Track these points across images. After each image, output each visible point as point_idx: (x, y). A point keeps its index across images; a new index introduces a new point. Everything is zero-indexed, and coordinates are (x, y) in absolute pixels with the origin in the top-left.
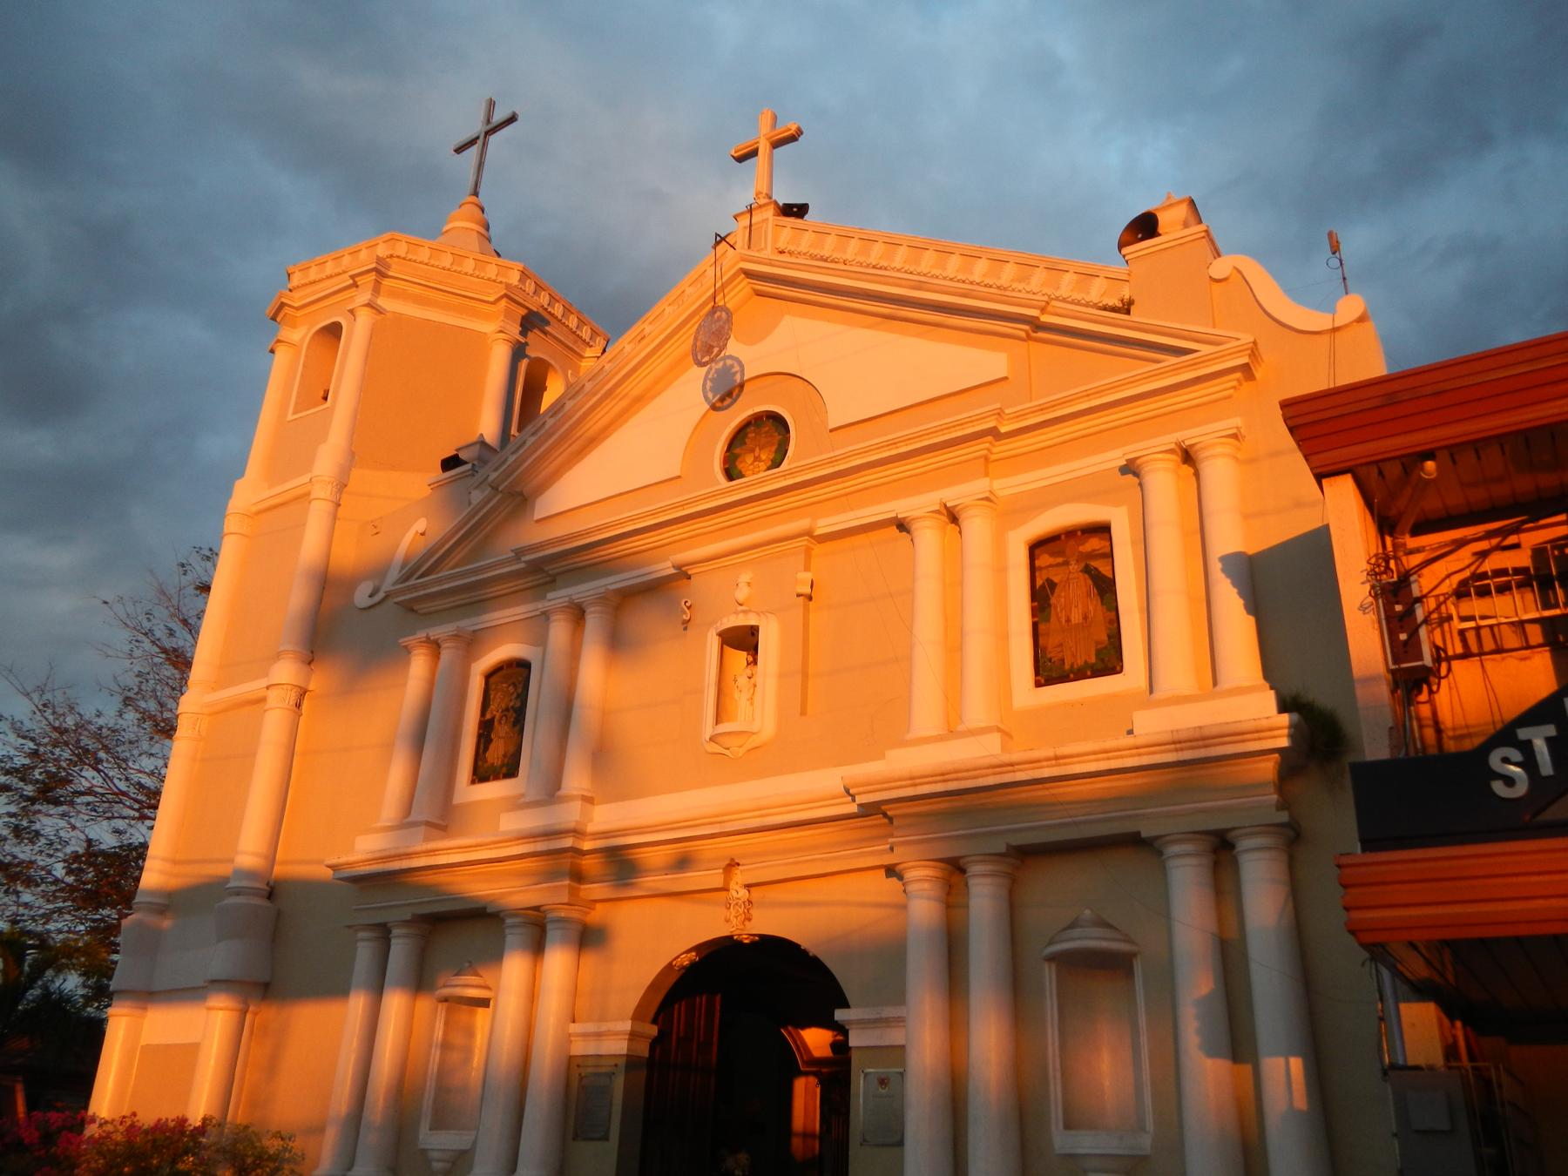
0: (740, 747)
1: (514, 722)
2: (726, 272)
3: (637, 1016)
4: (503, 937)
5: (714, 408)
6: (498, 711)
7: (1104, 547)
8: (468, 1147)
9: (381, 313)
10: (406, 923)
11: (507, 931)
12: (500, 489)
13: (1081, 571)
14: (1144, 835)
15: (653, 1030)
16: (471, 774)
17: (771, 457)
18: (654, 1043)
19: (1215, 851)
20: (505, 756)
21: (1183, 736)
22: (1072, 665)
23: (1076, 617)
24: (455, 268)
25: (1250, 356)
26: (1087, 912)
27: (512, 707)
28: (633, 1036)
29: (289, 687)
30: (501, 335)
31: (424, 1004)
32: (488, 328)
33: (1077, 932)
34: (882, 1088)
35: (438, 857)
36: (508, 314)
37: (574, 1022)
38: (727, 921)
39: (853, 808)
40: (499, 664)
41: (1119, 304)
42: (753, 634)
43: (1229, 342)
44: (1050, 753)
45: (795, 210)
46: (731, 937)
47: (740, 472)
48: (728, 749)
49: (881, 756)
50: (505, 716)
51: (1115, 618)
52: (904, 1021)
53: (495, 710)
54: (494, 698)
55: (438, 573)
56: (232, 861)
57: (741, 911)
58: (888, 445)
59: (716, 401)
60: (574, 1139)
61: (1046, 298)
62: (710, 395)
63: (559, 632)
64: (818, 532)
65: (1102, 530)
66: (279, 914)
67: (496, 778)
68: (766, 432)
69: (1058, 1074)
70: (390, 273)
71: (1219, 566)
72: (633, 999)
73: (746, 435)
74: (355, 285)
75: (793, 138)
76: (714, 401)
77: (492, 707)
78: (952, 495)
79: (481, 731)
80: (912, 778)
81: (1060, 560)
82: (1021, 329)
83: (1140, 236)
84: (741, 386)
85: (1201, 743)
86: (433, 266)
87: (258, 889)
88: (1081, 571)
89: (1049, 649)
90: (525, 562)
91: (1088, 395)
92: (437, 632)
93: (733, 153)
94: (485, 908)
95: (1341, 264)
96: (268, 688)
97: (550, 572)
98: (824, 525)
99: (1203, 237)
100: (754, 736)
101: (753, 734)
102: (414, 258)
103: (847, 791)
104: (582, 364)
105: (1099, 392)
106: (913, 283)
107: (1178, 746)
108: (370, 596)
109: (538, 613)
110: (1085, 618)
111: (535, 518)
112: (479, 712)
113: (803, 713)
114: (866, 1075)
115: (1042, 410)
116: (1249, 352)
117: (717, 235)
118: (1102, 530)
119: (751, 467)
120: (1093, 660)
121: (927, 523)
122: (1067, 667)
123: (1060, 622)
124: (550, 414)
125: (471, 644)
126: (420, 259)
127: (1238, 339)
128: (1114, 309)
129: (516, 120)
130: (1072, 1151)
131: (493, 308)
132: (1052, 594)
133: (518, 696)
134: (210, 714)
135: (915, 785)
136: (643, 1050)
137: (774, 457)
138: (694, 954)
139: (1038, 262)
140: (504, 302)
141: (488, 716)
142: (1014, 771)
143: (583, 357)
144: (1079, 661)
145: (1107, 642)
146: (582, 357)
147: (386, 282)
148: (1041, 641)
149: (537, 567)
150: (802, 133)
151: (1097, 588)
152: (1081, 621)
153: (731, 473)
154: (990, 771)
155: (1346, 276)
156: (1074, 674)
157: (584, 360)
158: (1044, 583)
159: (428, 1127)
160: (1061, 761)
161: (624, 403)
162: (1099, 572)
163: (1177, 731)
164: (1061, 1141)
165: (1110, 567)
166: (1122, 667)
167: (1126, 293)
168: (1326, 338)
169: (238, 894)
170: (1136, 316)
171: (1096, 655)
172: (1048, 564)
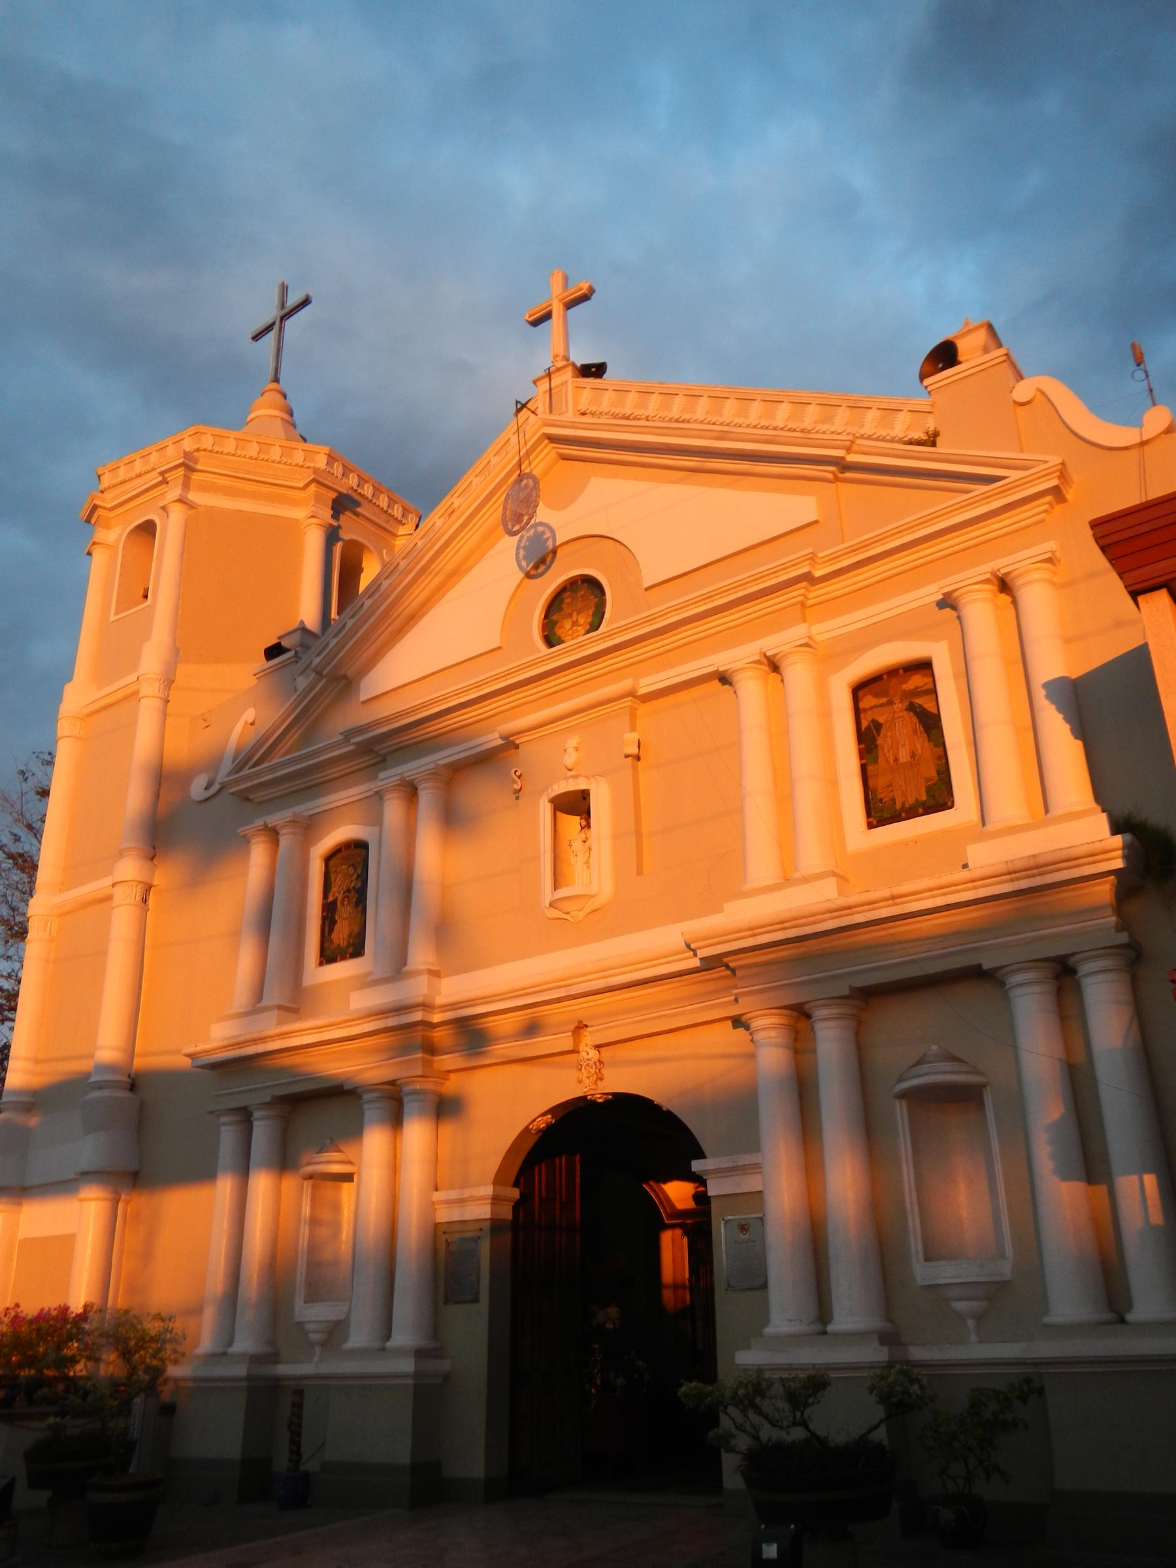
0: (580, 910)
2: (530, 439)
3: (498, 1181)
4: (361, 1113)
5: (528, 576)
6: (340, 892)
7: (928, 683)
8: (343, 1318)
9: (194, 508)
10: (265, 1105)
11: (366, 1106)
12: (324, 673)
13: (906, 710)
14: (986, 966)
15: (515, 1193)
17: (589, 620)
18: (517, 1206)
19: (1058, 977)
20: (350, 936)
21: (1018, 865)
22: (904, 803)
23: (904, 756)
24: (262, 456)
25: (1059, 478)
26: (934, 1047)
27: (353, 887)
28: (496, 1200)
29: (134, 884)
30: (313, 520)
31: (290, 1183)
32: (300, 513)
33: (926, 1067)
34: (744, 1234)
35: (292, 1039)
36: (318, 498)
37: (437, 1190)
38: (580, 1082)
39: (695, 963)
40: (337, 846)
41: (925, 437)
42: (584, 798)
43: (1038, 465)
44: (886, 893)
45: (593, 370)
46: (585, 1097)
47: (560, 638)
48: (568, 913)
49: (721, 910)
50: (347, 897)
51: (943, 753)
52: (760, 1168)
53: (336, 892)
54: (335, 880)
55: (270, 761)
56: (92, 1056)
57: (593, 1071)
58: (704, 599)
59: (530, 569)
60: (445, 1303)
61: (850, 437)
62: (524, 564)
63: (393, 810)
64: (641, 692)
65: (924, 666)
66: (142, 1106)
67: (343, 958)
68: (582, 596)
69: (916, 1208)
70: (199, 467)
71: (1043, 692)
72: (494, 1164)
73: (562, 601)
74: (165, 482)
75: (585, 298)
76: (528, 569)
78: (771, 643)
79: (325, 914)
80: (751, 929)
81: (884, 700)
82: (828, 471)
83: (940, 366)
84: (554, 552)
85: (1035, 871)
86: (240, 456)
87: (120, 1082)
88: (906, 710)
89: (880, 790)
90: (354, 744)
91: (899, 532)
92: (274, 819)
93: (527, 317)
94: (341, 1086)
95: (1147, 376)
96: (113, 885)
97: (380, 752)
98: (647, 685)
99: (1005, 361)
100: (594, 899)
101: (592, 896)
102: (221, 450)
103: (688, 946)
104: (397, 543)
105: (910, 528)
106: (717, 434)
107: (1013, 876)
108: (206, 789)
109: (371, 793)
110: (913, 756)
111: (362, 699)
113: (640, 872)
114: (726, 1222)
115: (854, 551)
116: (1058, 474)
117: (517, 402)
118: (924, 666)
119: (570, 632)
120: (924, 797)
121: (749, 673)
122: (898, 806)
123: (888, 762)
124: (368, 595)
125: (309, 828)
126: (226, 451)
127: (1047, 462)
128: (919, 443)
129: (310, 302)
130: (934, 1282)
131: (302, 494)
132: (879, 735)
133: (358, 877)
134: (61, 915)
136: (507, 1213)
137: (592, 621)
138: (549, 1116)
139: (841, 401)
140: (313, 487)
142: (852, 914)
143: (396, 536)
144: (910, 798)
145: (937, 778)
146: (396, 536)
148: (871, 783)
149: (367, 748)
150: (594, 292)
151: (923, 726)
152: (909, 759)
153: (550, 640)
154: (828, 915)
155: (1152, 386)
156: (907, 813)
157: (397, 539)
158: (869, 724)
159: (302, 1302)
160: (898, 900)
161: (438, 580)
162: (924, 709)
163: (1011, 861)
164: (923, 1273)
165: (934, 703)
166: (953, 802)
167: (931, 425)
168: (1135, 453)
169: (100, 1088)
170: (942, 448)
171: (927, 792)
172: (872, 705)
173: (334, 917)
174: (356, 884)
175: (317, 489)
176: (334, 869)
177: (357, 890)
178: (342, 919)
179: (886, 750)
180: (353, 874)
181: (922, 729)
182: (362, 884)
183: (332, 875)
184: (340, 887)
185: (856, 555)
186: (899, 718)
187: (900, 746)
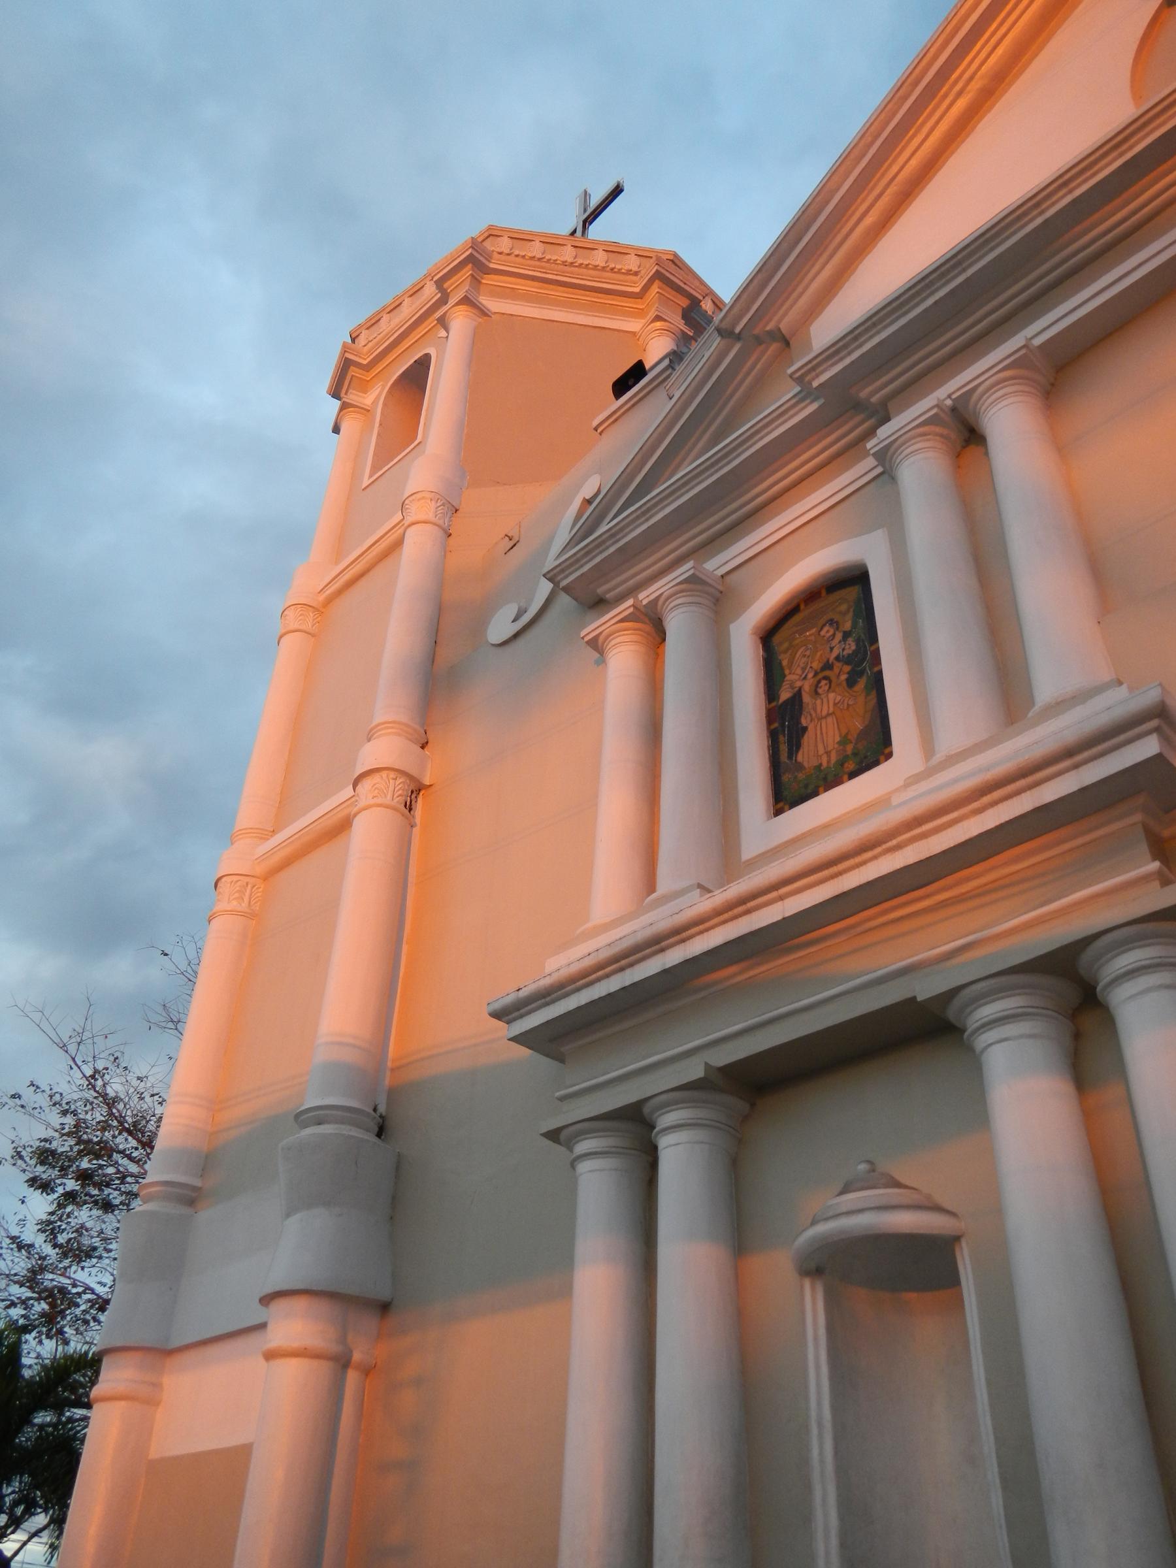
1: (847, 680)
6: (805, 678)
9: (486, 315)
16: (771, 801)
20: (844, 741)
27: (837, 658)
29: (392, 775)
30: (658, 324)
50: (825, 678)
54: (791, 663)
70: (492, 266)
77: (788, 678)
79: (776, 725)
112: (763, 696)
129: (622, 191)
133: (846, 635)
141: (785, 695)
147: (488, 280)
161: (962, 104)
173: (799, 722)
174: (843, 650)
175: (660, 291)
176: (786, 645)
177: (847, 660)
178: (820, 719)
180: (834, 635)
182: (857, 645)
183: (781, 657)
184: (804, 669)
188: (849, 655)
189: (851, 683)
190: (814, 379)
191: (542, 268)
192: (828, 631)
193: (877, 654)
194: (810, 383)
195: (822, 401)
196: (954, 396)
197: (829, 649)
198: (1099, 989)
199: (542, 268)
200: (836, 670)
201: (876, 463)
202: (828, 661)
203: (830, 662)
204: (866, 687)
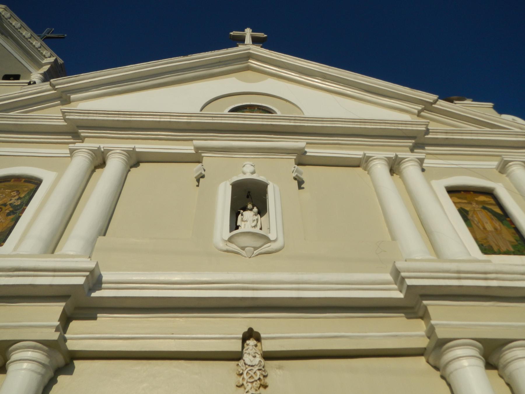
0: (256, 248)
1: (8, 213)
27: (10, 204)
48: (243, 248)
57: (257, 378)
58: (360, 122)
80: (459, 272)
110: (496, 229)
118: (489, 193)
133: (20, 198)
135: (459, 278)
152: (493, 230)
174: (14, 202)
179: (475, 222)
180: (15, 196)
181: (496, 218)
185: (446, 135)
186: (479, 211)
187: (485, 224)
188: (15, 205)
189: (8, 214)
190: (68, 115)
191: (14, 31)
192: (14, 194)
193: (24, 210)
194: (66, 115)
195: (65, 124)
196: (104, 148)
197: (10, 199)
198: (8, 362)
199: (14, 31)
200: (7, 208)
201: (69, 153)
202: (6, 203)
203: (7, 204)
204: (12, 219)
